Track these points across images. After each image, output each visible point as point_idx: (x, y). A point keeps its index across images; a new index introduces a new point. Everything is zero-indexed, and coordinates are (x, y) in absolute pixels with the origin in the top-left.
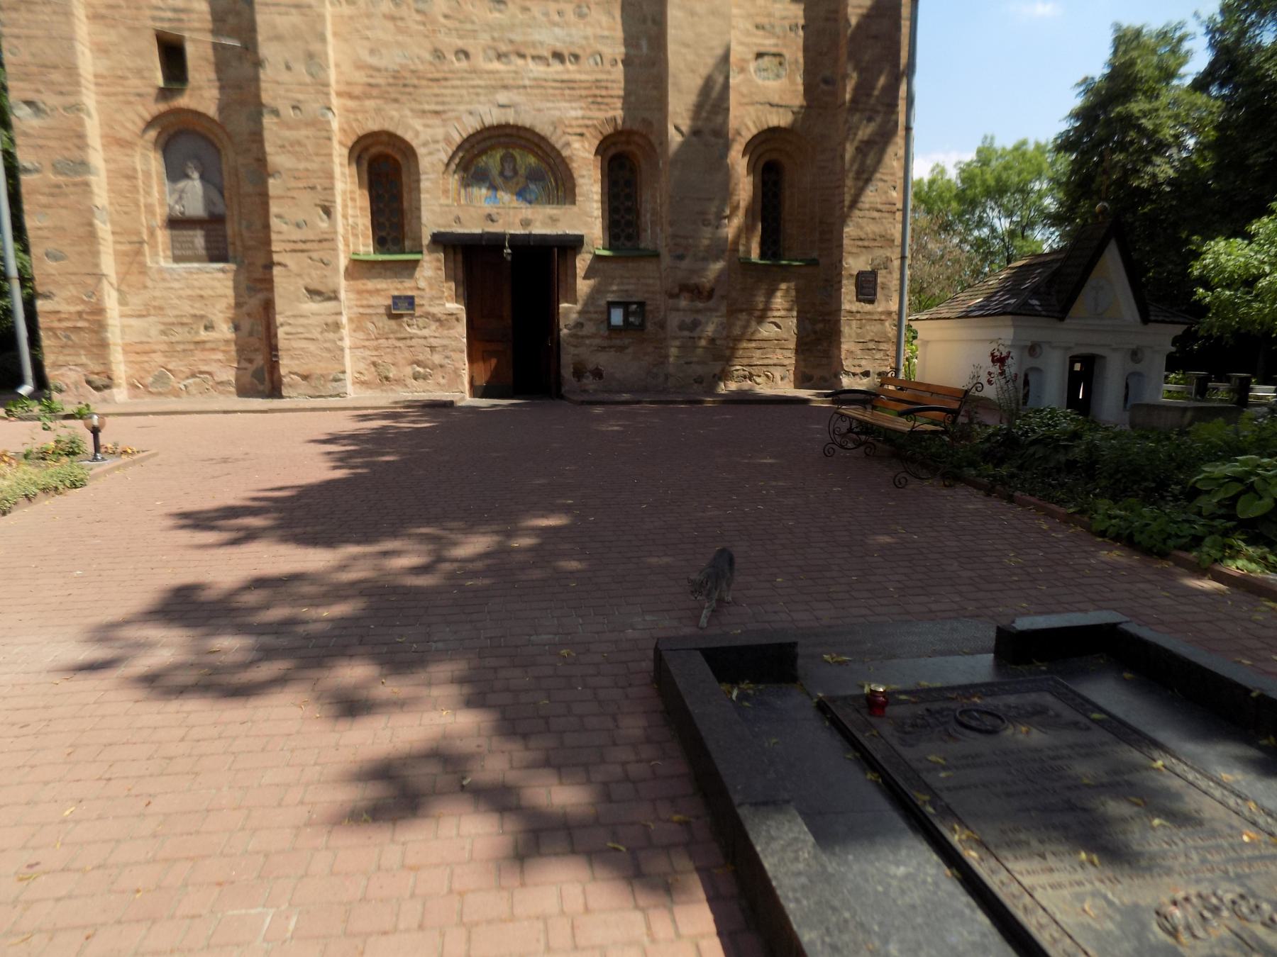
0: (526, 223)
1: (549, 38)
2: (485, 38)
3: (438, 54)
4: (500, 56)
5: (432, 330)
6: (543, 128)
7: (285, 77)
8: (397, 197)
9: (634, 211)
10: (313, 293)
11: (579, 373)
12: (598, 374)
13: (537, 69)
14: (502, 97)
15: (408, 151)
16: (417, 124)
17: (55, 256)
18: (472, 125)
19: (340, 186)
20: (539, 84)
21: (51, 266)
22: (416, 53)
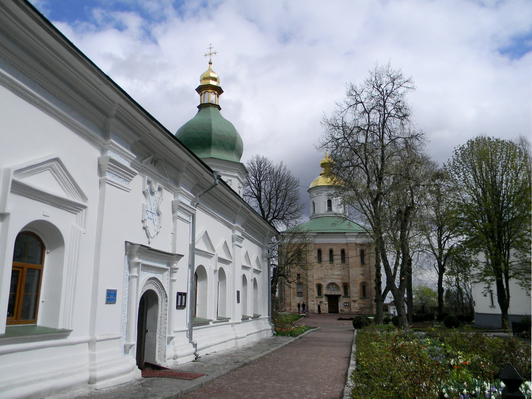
0: (335, 293)
1: (337, 273)
2: (330, 274)
3: (325, 275)
4: (331, 275)
5: (324, 305)
6: (337, 283)
7: (310, 278)
8: (321, 290)
9: (347, 291)
10: (312, 301)
11: (341, 310)
12: (343, 311)
13: (336, 277)
14: (332, 280)
15: (322, 285)
16: (323, 282)
17: (288, 296)
18: (329, 282)
19: (315, 289)
20: (336, 278)
21: (287, 297)
22: (323, 276)
